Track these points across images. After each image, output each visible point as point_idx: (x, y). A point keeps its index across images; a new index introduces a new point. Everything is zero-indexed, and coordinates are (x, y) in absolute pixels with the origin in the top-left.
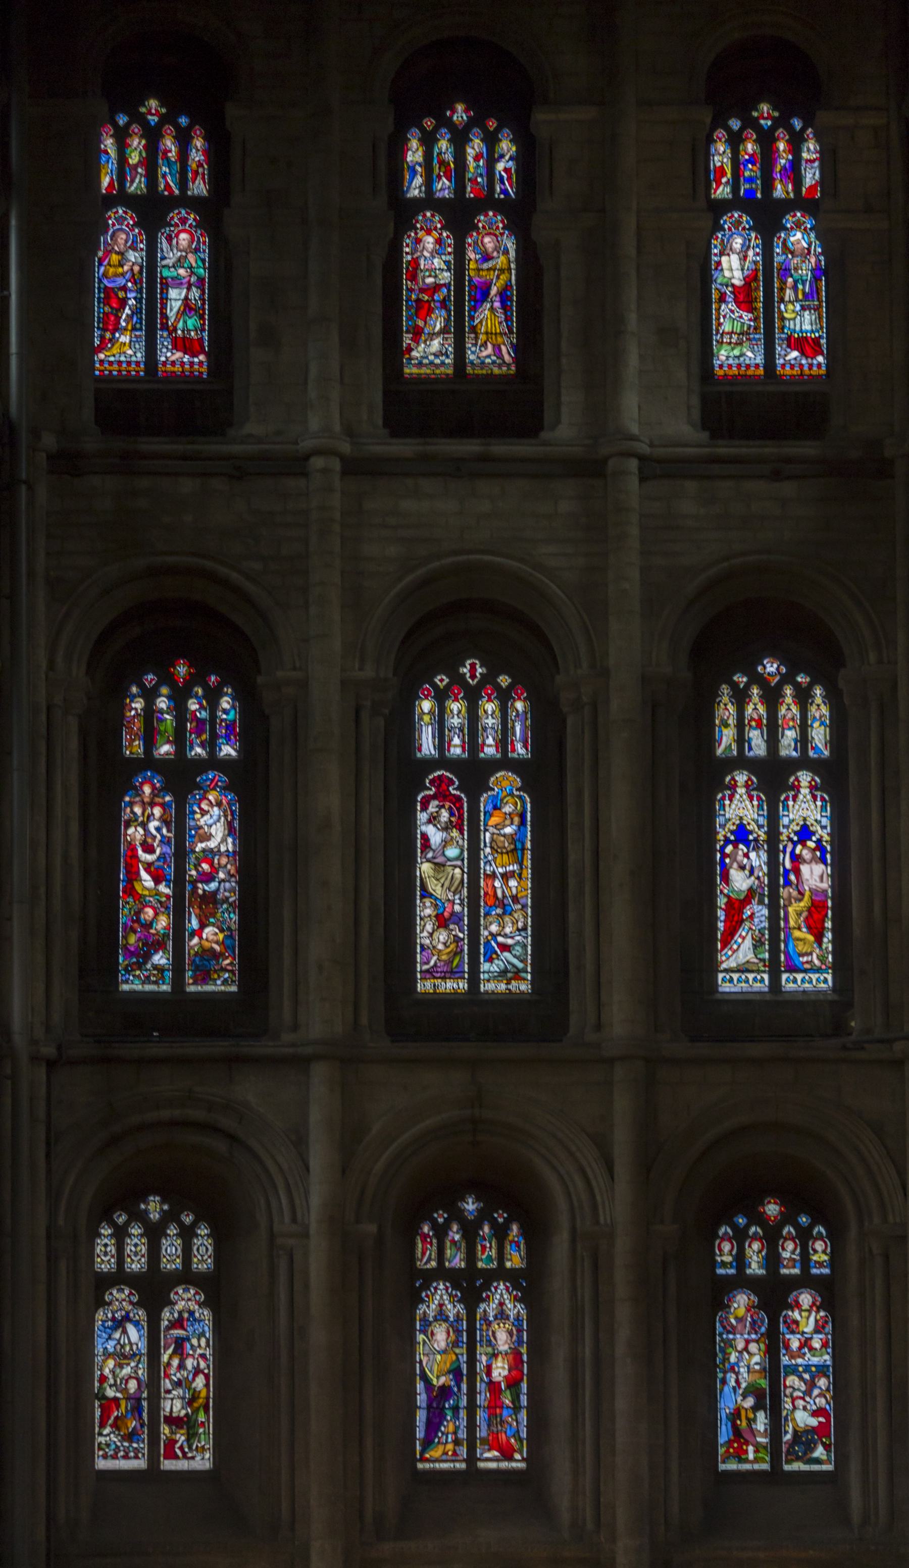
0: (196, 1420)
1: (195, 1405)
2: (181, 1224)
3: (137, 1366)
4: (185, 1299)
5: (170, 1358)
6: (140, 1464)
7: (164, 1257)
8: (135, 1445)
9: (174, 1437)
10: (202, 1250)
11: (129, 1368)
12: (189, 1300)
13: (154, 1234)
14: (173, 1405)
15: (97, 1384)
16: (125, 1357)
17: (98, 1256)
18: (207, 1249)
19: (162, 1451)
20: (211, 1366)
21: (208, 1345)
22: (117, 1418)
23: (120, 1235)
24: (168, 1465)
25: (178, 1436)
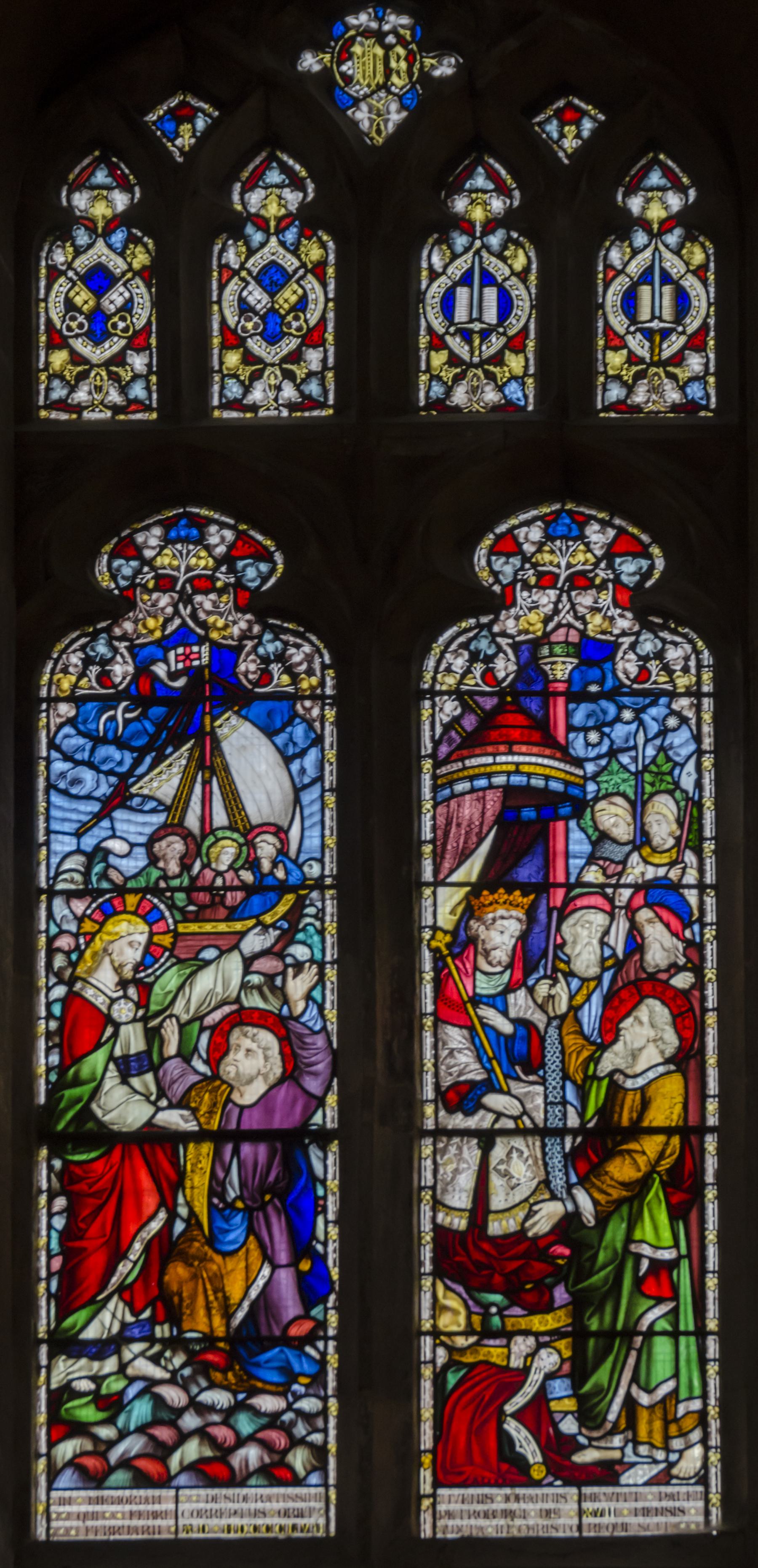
0: (626, 1254)
1: (622, 1170)
2: (531, 162)
3: (277, 952)
4: (559, 580)
5: (470, 910)
6: (304, 1509)
7: (437, 343)
8: (268, 1403)
9: (494, 1353)
10: (655, 303)
11: (233, 964)
12: (580, 581)
13: (378, 213)
14: (497, 1176)
15: (44, 1059)
16: (206, 900)
17: (57, 341)
18: (682, 300)
19: (427, 1440)
20: (711, 951)
21: (690, 837)
22: (164, 1249)
23: (184, 225)
24: (458, 1512)
25: (522, 1345)
